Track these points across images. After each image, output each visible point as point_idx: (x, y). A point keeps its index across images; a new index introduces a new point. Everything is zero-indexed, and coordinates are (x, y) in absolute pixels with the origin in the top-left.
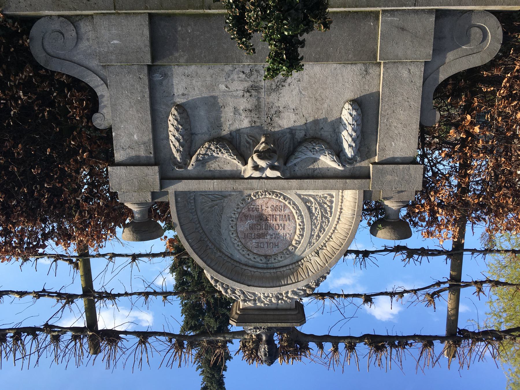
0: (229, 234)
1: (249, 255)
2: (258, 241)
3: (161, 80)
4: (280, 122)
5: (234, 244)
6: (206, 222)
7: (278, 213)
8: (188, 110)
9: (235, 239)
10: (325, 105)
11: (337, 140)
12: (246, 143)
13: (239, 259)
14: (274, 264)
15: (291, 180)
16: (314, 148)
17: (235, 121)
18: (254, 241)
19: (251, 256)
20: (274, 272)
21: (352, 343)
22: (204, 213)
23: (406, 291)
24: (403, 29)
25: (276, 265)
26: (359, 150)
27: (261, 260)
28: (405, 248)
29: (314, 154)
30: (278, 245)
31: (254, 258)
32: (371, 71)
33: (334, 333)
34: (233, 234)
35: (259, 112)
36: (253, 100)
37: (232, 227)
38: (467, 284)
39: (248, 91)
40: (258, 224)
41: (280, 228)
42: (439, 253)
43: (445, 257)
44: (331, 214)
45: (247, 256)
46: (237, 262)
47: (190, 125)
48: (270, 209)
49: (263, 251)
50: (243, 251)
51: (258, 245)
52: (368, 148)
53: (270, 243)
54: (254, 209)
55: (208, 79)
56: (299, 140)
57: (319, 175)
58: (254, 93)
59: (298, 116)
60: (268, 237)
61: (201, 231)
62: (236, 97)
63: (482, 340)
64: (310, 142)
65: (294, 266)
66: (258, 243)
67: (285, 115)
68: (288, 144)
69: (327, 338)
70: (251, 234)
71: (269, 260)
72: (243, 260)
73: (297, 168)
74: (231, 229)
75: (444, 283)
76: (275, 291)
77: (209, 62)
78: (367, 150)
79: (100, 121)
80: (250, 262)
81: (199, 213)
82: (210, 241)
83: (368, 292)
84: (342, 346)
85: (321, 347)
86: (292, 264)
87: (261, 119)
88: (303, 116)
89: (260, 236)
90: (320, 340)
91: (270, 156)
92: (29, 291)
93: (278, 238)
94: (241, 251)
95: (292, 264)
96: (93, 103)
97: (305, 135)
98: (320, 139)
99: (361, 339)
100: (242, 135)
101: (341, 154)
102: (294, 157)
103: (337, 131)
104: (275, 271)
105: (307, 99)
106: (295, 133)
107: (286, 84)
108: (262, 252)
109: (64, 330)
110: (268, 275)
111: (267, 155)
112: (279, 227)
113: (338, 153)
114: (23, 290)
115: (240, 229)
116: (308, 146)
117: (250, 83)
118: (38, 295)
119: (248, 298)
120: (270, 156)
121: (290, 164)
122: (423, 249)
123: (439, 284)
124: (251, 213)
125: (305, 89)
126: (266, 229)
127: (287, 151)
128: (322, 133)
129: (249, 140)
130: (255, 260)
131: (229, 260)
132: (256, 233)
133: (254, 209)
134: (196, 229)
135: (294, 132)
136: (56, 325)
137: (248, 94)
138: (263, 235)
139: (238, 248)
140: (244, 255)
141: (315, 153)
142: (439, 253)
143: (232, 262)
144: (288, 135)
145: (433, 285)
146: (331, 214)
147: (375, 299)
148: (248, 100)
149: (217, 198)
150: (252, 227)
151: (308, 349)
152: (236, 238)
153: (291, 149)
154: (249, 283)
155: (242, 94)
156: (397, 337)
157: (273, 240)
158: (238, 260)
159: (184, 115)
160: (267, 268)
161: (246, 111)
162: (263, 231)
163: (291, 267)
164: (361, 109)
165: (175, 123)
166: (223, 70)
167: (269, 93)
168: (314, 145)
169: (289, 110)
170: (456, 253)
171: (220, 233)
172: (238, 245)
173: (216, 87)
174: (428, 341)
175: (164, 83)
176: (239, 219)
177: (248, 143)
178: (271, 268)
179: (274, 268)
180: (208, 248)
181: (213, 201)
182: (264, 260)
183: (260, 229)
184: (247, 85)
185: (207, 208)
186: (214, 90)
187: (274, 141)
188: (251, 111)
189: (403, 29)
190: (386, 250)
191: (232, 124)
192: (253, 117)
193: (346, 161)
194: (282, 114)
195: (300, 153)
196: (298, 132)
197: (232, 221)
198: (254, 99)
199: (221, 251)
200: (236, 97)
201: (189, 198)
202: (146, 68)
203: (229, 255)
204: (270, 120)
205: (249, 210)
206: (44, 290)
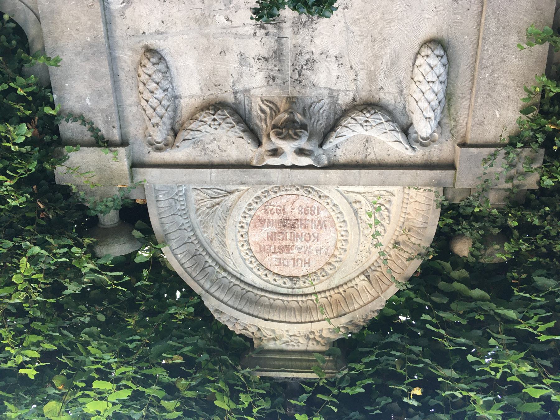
0: (237, 246)
1: (266, 275)
2: (279, 256)
3: (122, 8)
4: (314, 78)
5: (245, 259)
6: (204, 227)
7: (309, 217)
8: (168, 58)
9: (247, 254)
10: (388, 50)
11: (404, 107)
12: (259, 112)
13: (252, 281)
14: (304, 290)
15: (330, 171)
16: (366, 121)
17: (242, 76)
18: (274, 256)
19: (270, 278)
20: (302, 301)
22: (200, 215)
25: (307, 291)
26: (439, 123)
27: (285, 283)
29: (366, 130)
30: (309, 263)
31: (275, 280)
34: (243, 246)
35: (280, 61)
36: (271, 42)
37: (242, 236)
40: (279, 233)
41: (312, 238)
44: (389, 220)
45: (264, 277)
46: (250, 285)
47: (171, 82)
48: (296, 211)
49: (288, 271)
50: (258, 270)
51: (280, 262)
52: (455, 120)
53: (298, 260)
54: (274, 210)
56: (344, 108)
57: (375, 162)
59: (342, 69)
60: (295, 251)
61: (196, 242)
62: (242, 37)
64: (361, 111)
65: (332, 292)
66: (280, 259)
68: (325, 114)
70: (270, 246)
71: (295, 284)
72: (259, 283)
73: (339, 152)
74: (241, 239)
78: (453, 123)
80: (269, 285)
81: (193, 215)
82: (210, 256)
86: (329, 290)
87: (283, 74)
88: (351, 68)
89: (282, 250)
91: (296, 134)
93: (309, 253)
94: (255, 270)
95: (329, 290)
97: (354, 100)
100: (253, 99)
101: (410, 131)
102: (334, 135)
103: (405, 91)
104: (304, 298)
105: (358, 39)
106: (338, 95)
110: (294, 304)
111: (291, 132)
112: (310, 237)
115: (252, 239)
116: (357, 118)
119: (265, 337)
120: (296, 134)
121: (328, 146)
124: (269, 216)
125: (355, 22)
126: (291, 240)
127: (324, 125)
128: (382, 95)
129: (264, 107)
130: (276, 283)
131: (238, 283)
132: (277, 245)
133: (274, 210)
134: (189, 238)
135: (335, 94)
137: (263, 31)
139: (250, 266)
140: (259, 276)
141: (369, 128)
143: (242, 285)
144: (326, 100)
146: (389, 220)
148: (263, 41)
149: (219, 193)
150: (270, 237)
152: (248, 252)
153: (331, 122)
154: (266, 317)
155: (253, 32)
158: (250, 282)
159: (161, 67)
160: (293, 295)
161: (259, 59)
163: (328, 294)
164: (447, 56)
167: (296, 29)
168: (368, 115)
169: (328, 59)
171: (223, 244)
172: (251, 262)
173: (209, 20)
175: (128, 12)
176: (252, 225)
177: (263, 111)
178: (297, 295)
179: (302, 295)
180: (207, 265)
181: (212, 198)
182: (289, 284)
183: (283, 239)
185: (205, 208)
186: (207, 24)
187: (304, 109)
188: (266, 60)
191: (238, 81)
192: (272, 70)
193: (417, 141)
194: (317, 66)
195: (345, 129)
196: (342, 94)
197: (242, 227)
198: (273, 40)
199: (225, 270)
200: (242, 37)
201: (177, 194)
203: (238, 275)
204: (297, 75)
205: (266, 212)
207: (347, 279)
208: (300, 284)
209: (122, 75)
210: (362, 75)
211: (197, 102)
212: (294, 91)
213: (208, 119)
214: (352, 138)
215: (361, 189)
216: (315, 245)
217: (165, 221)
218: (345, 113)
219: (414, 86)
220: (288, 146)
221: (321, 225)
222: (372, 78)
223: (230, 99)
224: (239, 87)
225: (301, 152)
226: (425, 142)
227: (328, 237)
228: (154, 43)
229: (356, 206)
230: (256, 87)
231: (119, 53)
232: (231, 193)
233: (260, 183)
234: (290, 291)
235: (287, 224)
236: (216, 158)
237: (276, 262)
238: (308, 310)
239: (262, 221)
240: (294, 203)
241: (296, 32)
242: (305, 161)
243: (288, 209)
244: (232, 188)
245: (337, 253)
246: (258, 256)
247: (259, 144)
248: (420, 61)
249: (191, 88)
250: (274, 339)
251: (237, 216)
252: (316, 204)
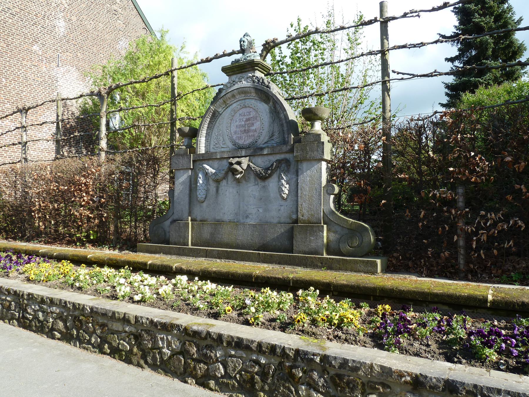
7: (239, 135)
104: (240, 99)
108: (248, 110)
113: (206, 175)
115: (259, 123)
144: (229, 183)
150: (253, 124)
157: (242, 117)
165: (283, 189)
207: (226, 110)
208: (242, 105)
215: (223, 149)
216: (237, 123)
229: (224, 143)
232: (266, 143)
237: (251, 113)
243: (246, 138)
245: (230, 121)
246: (258, 115)
248: (204, 196)
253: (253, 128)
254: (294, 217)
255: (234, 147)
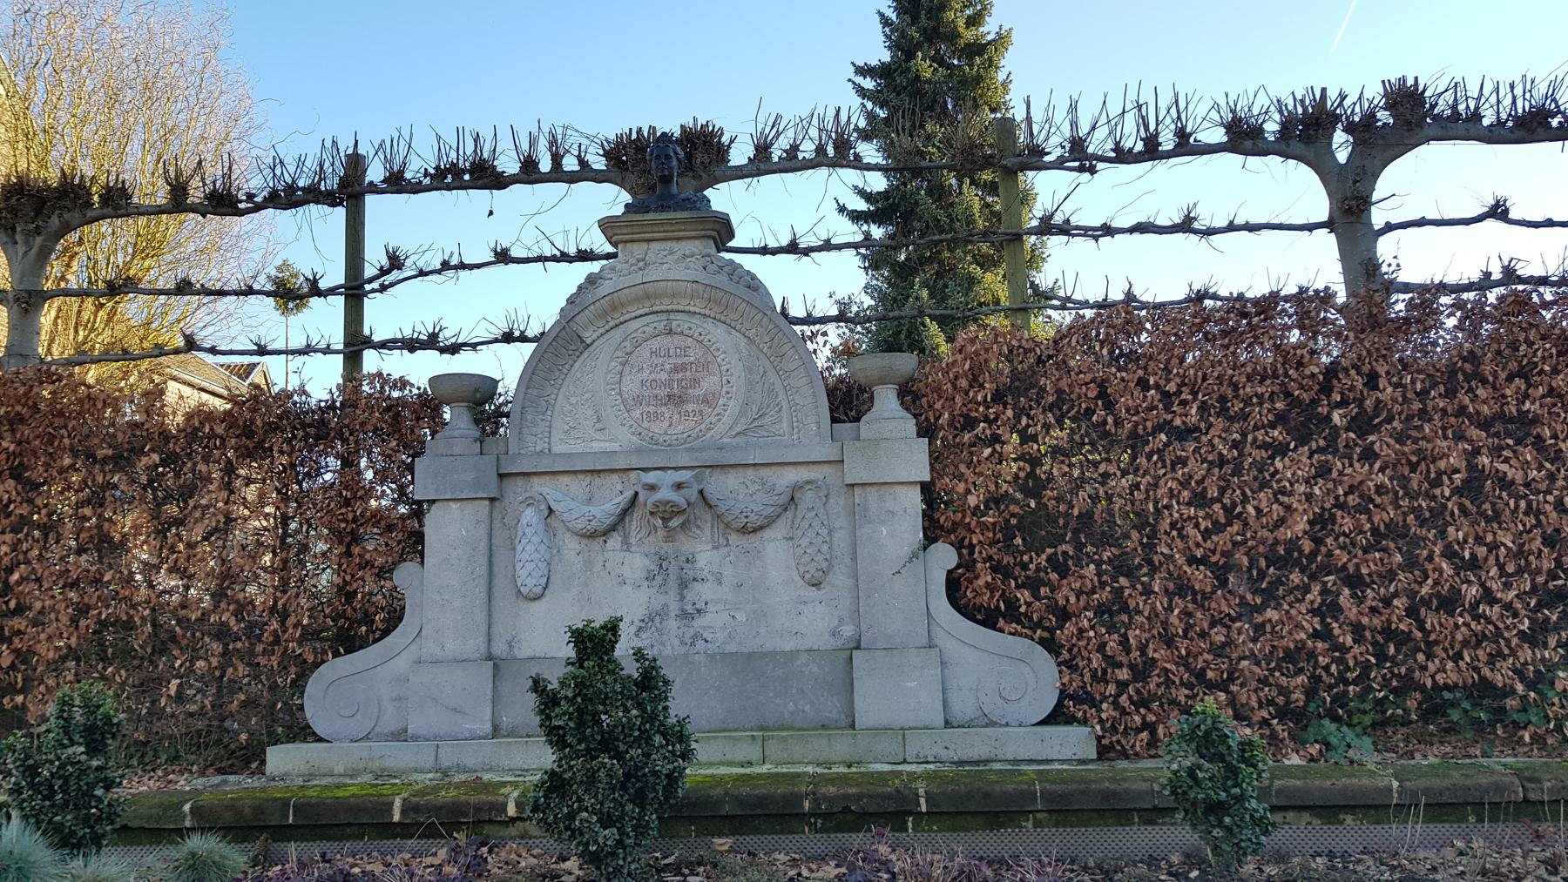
4: (647, 562)
7: (652, 409)
21: (529, 172)
23: (438, 272)
24: (455, 710)
25: (653, 317)
28: (443, 351)
32: (505, 647)
33: (562, 187)
38: (332, 291)
39: (699, 611)
42: (383, 345)
43: (376, 338)
55: (762, 630)
57: (581, 477)
58: (690, 609)
59: (619, 571)
63: (303, 189)
67: (640, 574)
69: (572, 178)
72: (709, 326)
73: (619, 487)
75: (373, 291)
76: (653, 274)
77: (763, 655)
79: (945, 556)
83: (501, 267)
84: (545, 166)
85: (582, 162)
90: (585, 173)
92: (1127, 236)
96: (954, 586)
98: (583, 536)
99: (514, 180)
104: (656, 308)
107: (638, 624)
109: (1059, 164)
114: (1136, 236)
117: (695, 624)
118: (1108, 230)
121: (629, 494)
122: (412, 350)
123: (383, 288)
136: (1075, 174)
138: (676, 369)
142: (383, 345)
144: (633, 541)
145: (392, 285)
147: (490, 257)
150: (696, 381)
151: (606, 154)
156: (449, 188)
162: (676, 377)
166: (740, 644)
170: (356, 343)
171: (749, 370)
174: (396, 183)
184: (699, 622)
189: (455, 710)
190: (474, 346)
202: (863, 645)
205: (701, 412)
206: (1096, 238)
207: (607, 336)
208: (661, 326)
209: (847, 560)
210: (599, 566)
211: (768, 534)
212: (667, 548)
213: (753, 517)
214: (612, 496)
217: (810, 400)
218: (613, 528)
219: (547, 556)
220: (665, 494)
221: (638, 400)
222: (589, 564)
223: (734, 538)
224: (724, 551)
225: (652, 488)
226: (530, 502)
227: (630, 386)
228: (812, 593)
230: (704, 551)
231: (849, 582)
233: (702, 449)
234: (672, 316)
235: (676, 400)
236: (750, 472)
238: (648, 297)
239: (706, 401)
240: (672, 426)
241: (665, 606)
242: (650, 478)
244: (741, 440)
245: (619, 368)
247: (701, 492)
249: (774, 546)
250: (685, 256)
251: (733, 407)
252: (646, 424)
253: (698, 392)
254: (848, 630)
255: (635, 439)
